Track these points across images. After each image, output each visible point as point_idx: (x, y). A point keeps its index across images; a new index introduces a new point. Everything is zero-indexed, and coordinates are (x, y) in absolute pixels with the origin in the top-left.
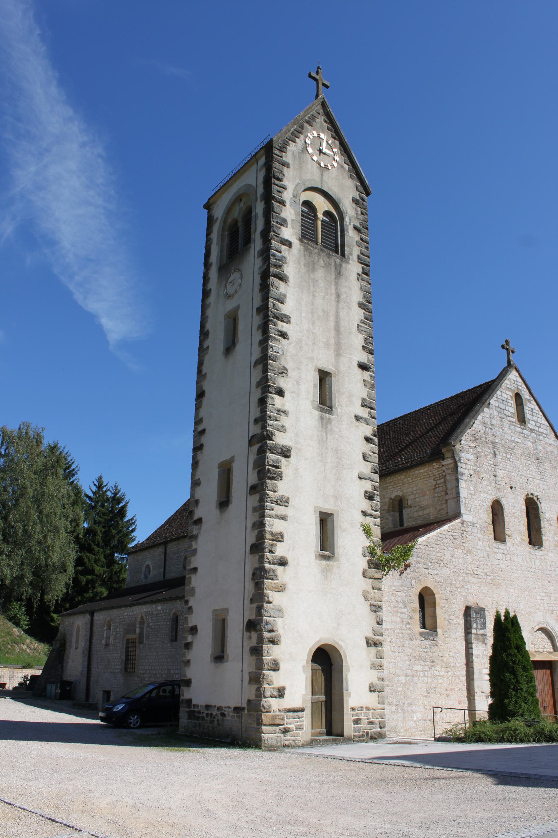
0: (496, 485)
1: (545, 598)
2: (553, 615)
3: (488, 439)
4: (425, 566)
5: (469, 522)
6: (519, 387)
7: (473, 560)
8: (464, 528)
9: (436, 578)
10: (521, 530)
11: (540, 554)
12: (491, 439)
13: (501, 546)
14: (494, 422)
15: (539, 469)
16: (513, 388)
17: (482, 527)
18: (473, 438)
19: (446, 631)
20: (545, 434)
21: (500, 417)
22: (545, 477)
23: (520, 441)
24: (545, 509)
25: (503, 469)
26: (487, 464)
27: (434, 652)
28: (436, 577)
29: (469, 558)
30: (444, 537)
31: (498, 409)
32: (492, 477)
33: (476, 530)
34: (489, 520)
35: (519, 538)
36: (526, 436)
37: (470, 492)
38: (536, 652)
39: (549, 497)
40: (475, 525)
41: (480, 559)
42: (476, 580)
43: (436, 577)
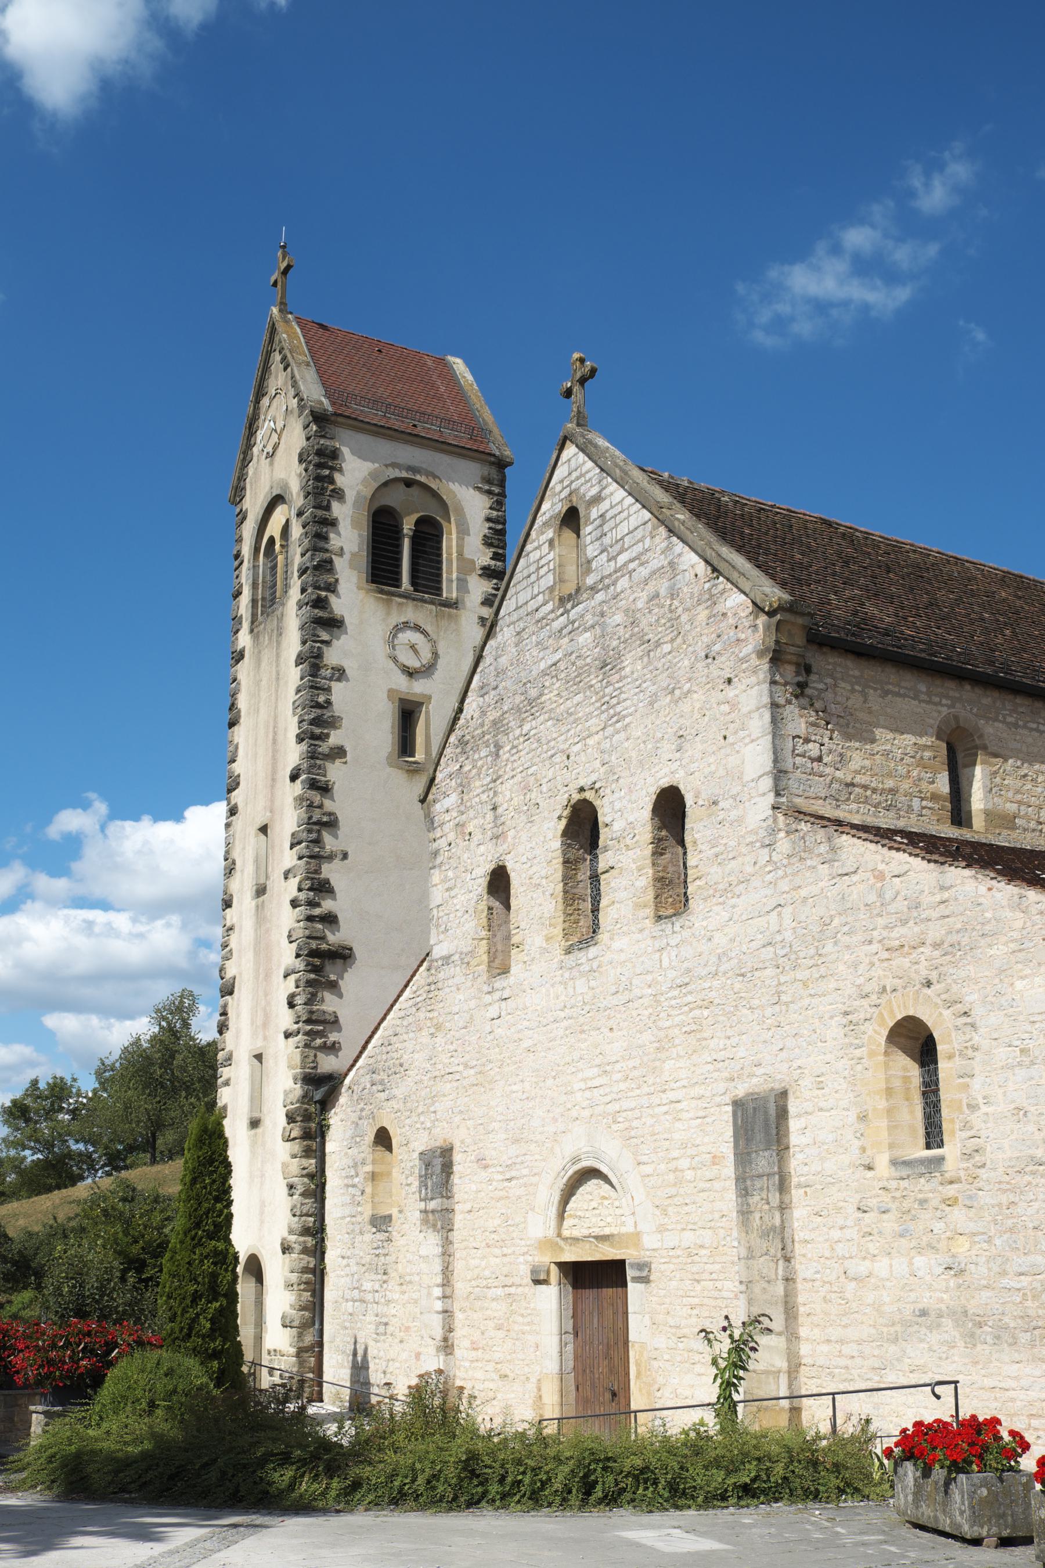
2: (615, 1127)
42: (448, 1085)
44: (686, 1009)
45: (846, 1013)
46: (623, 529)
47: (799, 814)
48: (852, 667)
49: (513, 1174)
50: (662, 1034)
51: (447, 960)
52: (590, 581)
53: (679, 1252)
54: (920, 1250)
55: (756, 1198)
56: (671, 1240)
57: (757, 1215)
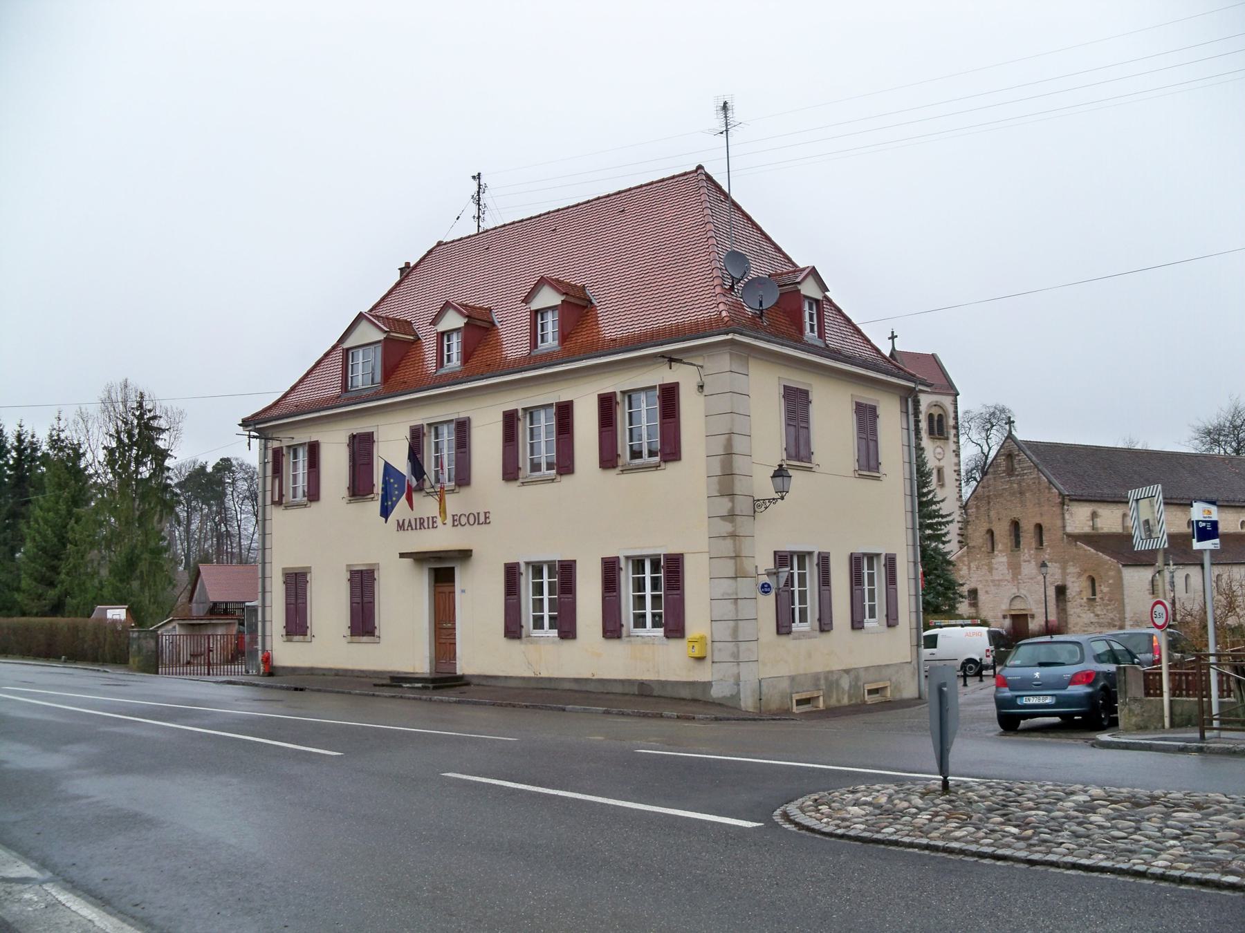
46: (1025, 465)
47: (1069, 535)
48: (1076, 503)
51: (974, 547)
52: (1017, 473)
54: (1092, 613)
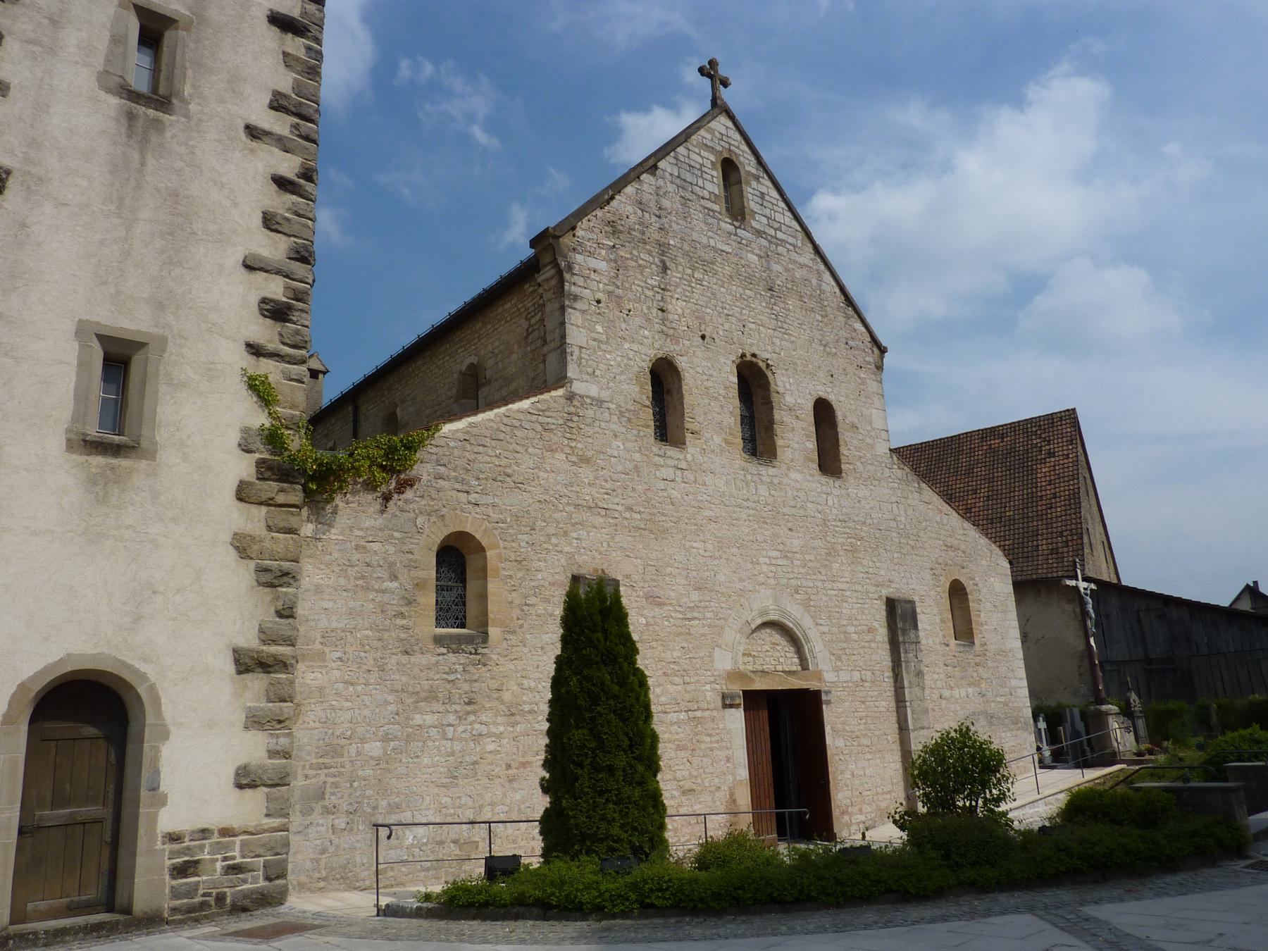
0: (664, 328)
1: (780, 562)
2: (798, 596)
3: (648, 234)
4: (458, 486)
5: (588, 397)
6: (732, 148)
7: (596, 478)
8: (572, 410)
9: (491, 514)
10: (725, 424)
11: (770, 473)
12: (656, 236)
13: (672, 452)
14: (666, 203)
15: (772, 309)
16: (719, 148)
17: (624, 410)
18: (608, 229)
19: (514, 632)
20: (790, 244)
21: (681, 197)
22: (785, 326)
23: (730, 251)
24: (784, 387)
25: (684, 298)
26: (643, 285)
27: (476, 681)
28: (490, 511)
29: (585, 473)
30: (517, 424)
31: (678, 181)
32: (654, 311)
33: (606, 415)
34: (644, 397)
35: (718, 440)
36: (744, 242)
37: (596, 336)
38: (754, 672)
39: (795, 364)
40: (605, 405)
41: (615, 477)
42: (601, 520)
43: (490, 511)
44: (846, 536)
45: (932, 569)
49: (696, 615)
50: (829, 545)
53: (850, 685)
55: (911, 655)
56: (844, 676)
57: (913, 664)
